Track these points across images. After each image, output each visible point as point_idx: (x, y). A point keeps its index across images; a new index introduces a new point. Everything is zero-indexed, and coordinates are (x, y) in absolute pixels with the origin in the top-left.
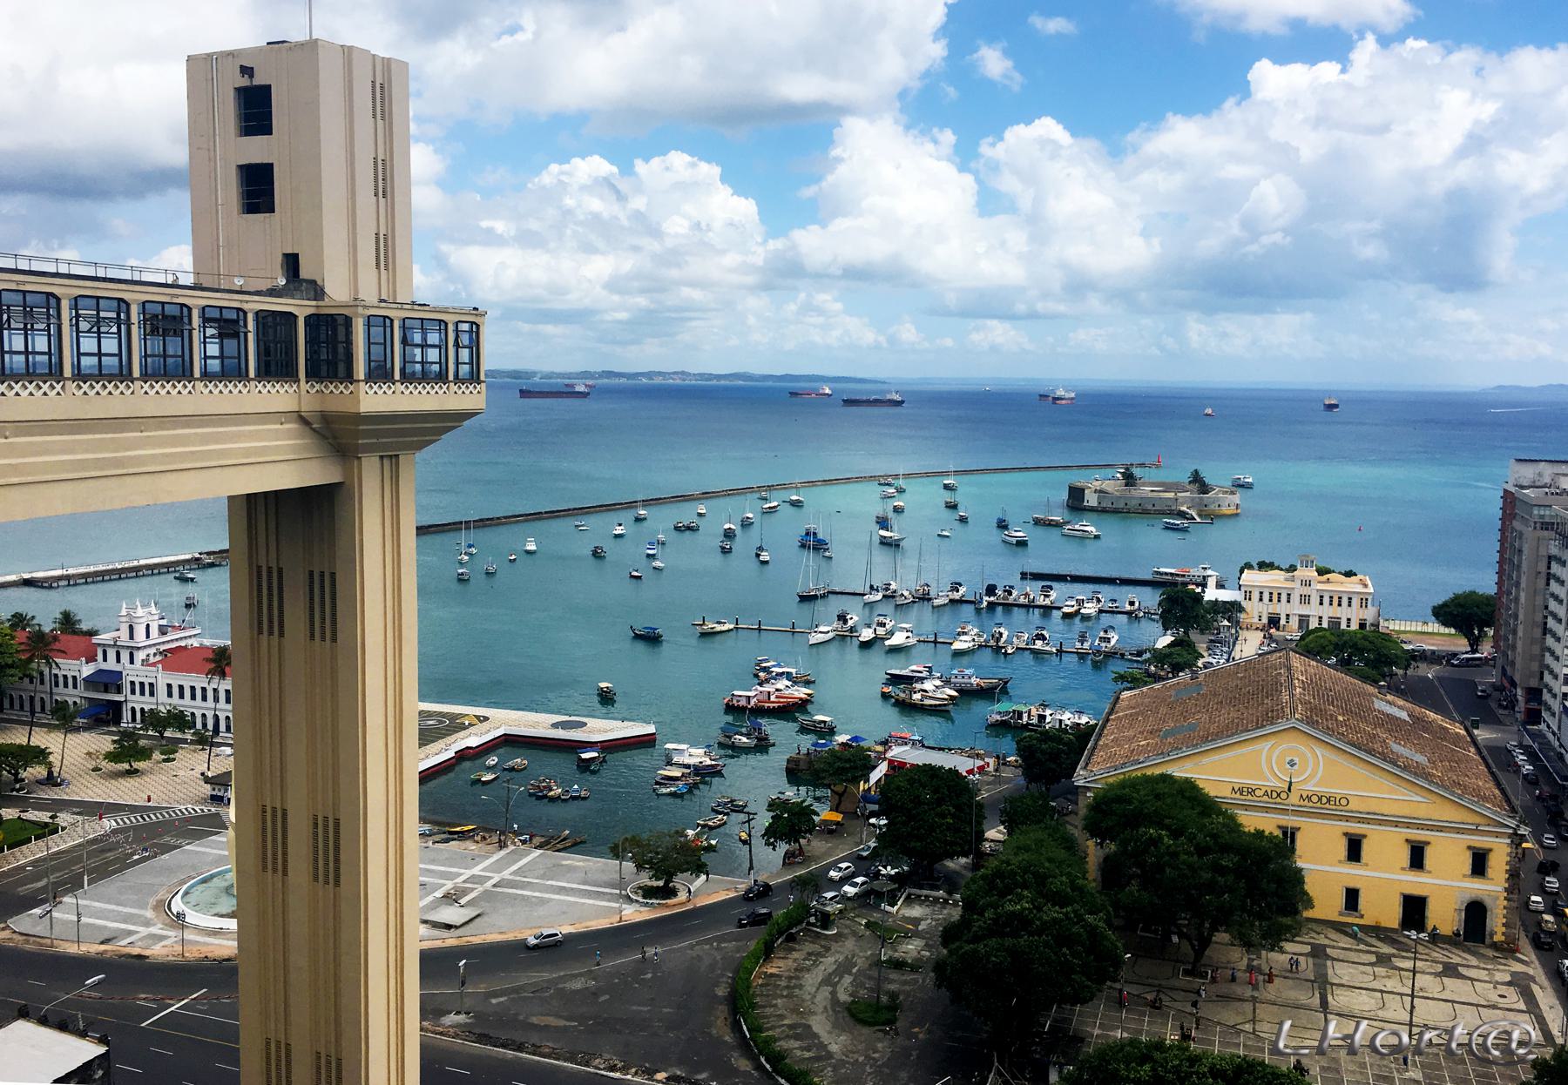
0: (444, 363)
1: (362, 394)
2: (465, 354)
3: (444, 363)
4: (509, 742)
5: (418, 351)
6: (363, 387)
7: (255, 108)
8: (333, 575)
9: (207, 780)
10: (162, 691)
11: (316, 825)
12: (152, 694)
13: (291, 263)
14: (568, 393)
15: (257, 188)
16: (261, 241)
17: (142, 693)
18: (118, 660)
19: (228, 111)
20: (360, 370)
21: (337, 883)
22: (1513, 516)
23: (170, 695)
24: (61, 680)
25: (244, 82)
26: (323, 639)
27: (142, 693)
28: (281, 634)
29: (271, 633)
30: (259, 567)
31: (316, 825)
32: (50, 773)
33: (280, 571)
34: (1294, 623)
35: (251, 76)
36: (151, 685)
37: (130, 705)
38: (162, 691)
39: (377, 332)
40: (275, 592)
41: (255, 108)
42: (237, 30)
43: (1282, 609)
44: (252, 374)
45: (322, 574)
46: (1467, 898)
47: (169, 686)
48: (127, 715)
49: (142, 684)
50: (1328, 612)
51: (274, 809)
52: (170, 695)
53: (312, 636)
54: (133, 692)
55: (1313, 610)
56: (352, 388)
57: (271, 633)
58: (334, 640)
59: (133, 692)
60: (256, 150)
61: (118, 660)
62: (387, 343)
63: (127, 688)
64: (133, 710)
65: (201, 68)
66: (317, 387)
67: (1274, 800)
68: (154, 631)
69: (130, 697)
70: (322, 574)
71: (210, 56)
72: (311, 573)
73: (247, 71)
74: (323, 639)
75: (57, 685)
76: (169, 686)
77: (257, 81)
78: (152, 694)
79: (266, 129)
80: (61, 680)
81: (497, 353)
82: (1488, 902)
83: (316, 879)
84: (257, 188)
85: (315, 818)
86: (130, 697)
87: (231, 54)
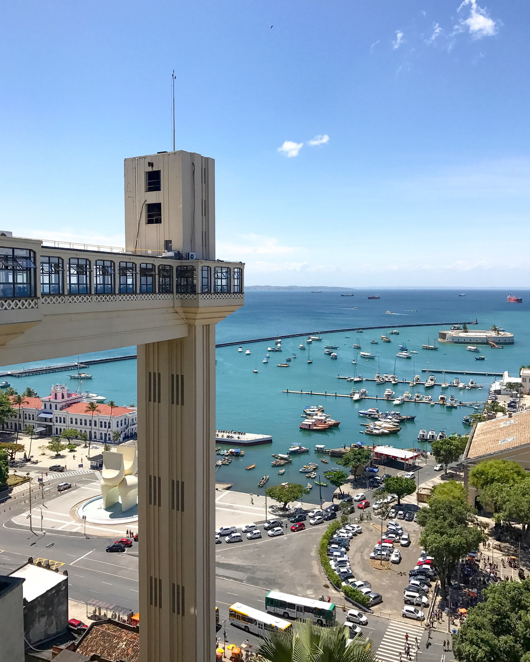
0: (229, 285)
1: (200, 299)
2: (236, 282)
3: (229, 285)
5: (219, 281)
6: (200, 296)
7: (154, 181)
8: (182, 376)
9: (89, 459)
10: (68, 421)
11: (173, 485)
12: (64, 422)
13: (168, 245)
15: (154, 214)
17: (61, 422)
18: (51, 408)
20: (199, 290)
21: (183, 510)
23: (72, 423)
24: (28, 416)
25: (150, 169)
26: (178, 403)
27: (61, 422)
28: (159, 402)
29: (155, 401)
30: (150, 374)
31: (173, 485)
32: (25, 455)
33: (159, 374)
35: (152, 166)
36: (64, 418)
37: (55, 427)
38: (68, 421)
39: (205, 273)
41: (154, 181)
42: (149, 148)
44: (157, 292)
45: (177, 376)
47: (71, 419)
48: (54, 431)
51: (155, 477)
52: (72, 423)
54: (57, 421)
56: (195, 297)
57: (155, 401)
58: (182, 404)
59: (57, 421)
60: (153, 197)
61: (51, 408)
62: (209, 278)
63: (54, 420)
64: (57, 429)
65: (130, 164)
66: (180, 297)
68: (66, 396)
69: (55, 423)
70: (177, 376)
71: (134, 158)
73: (151, 164)
74: (178, 403)
75: (26, 418)
76: (71, 419)
77: (155, 169)
78: (64, 422)
79: (158, 189)
80: (28, 416)
81: (250, 280)
83: (173, 508)
84: (154, 214)
85: (173, 481)
86: (55, 423)
87: (145, 157)
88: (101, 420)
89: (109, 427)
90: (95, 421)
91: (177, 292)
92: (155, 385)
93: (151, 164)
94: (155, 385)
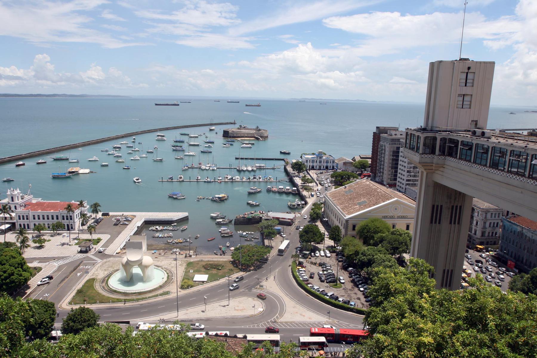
4: (148, 223)
8: (461, 207)
10: (31, 217)
12: (27, 219)
22: (379, 140)
23: (34, 218)
34: (318, 167)
36: (27, 216)
38: (31, 217)
40: (454, 212)
43: (315, 164)
49: (23, 216)
50: (325, 165)
52: (34, 218)
67: (392, 217)
70: (457, 207)
76: (34, 216)
78: (27, 219)
88: (62, 215)
89: (71, 219)
90: (57, 216)
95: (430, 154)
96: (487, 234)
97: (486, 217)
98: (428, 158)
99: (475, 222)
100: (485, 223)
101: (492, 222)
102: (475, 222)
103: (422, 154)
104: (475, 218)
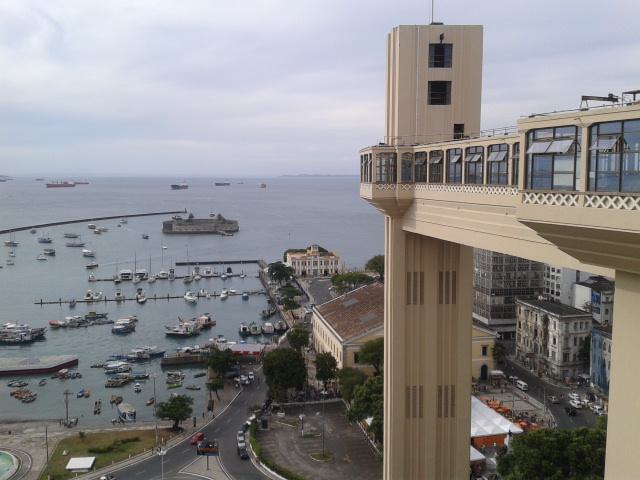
7: (440, 54)
8: (454, 273)
11: (440, 391)
13: (459, 129)
14: (66, 185)
15: (439, 93)
16: (443, 116)
19: (424, 55)
26: (447, 302)
28: (422, 302)
33: (422, 274)
34: (312, 273)
41: (440, 54)
46: (482, 364)
50: (323, 267)
53: (441, 302)
55: (318, 267)
58: (454, 302)
60: (440, 74)
70: (448, 273)
72: (441, 274)
74: (447, 302)
77: (444, 42)
82: (488, 365)
84: (439, 93)
91: (487, 182)
92: (415, 286)
93: (442, 37)
94: (415, 286)
95: (388, 182)
96: (571, 358)
97: (567, 331)
98: (387, 191)
99: (551, 340)
100: (566, 339)
101: (579, 336)
102: (551, 340)
103: (377, 183)
104: (550, 333)
